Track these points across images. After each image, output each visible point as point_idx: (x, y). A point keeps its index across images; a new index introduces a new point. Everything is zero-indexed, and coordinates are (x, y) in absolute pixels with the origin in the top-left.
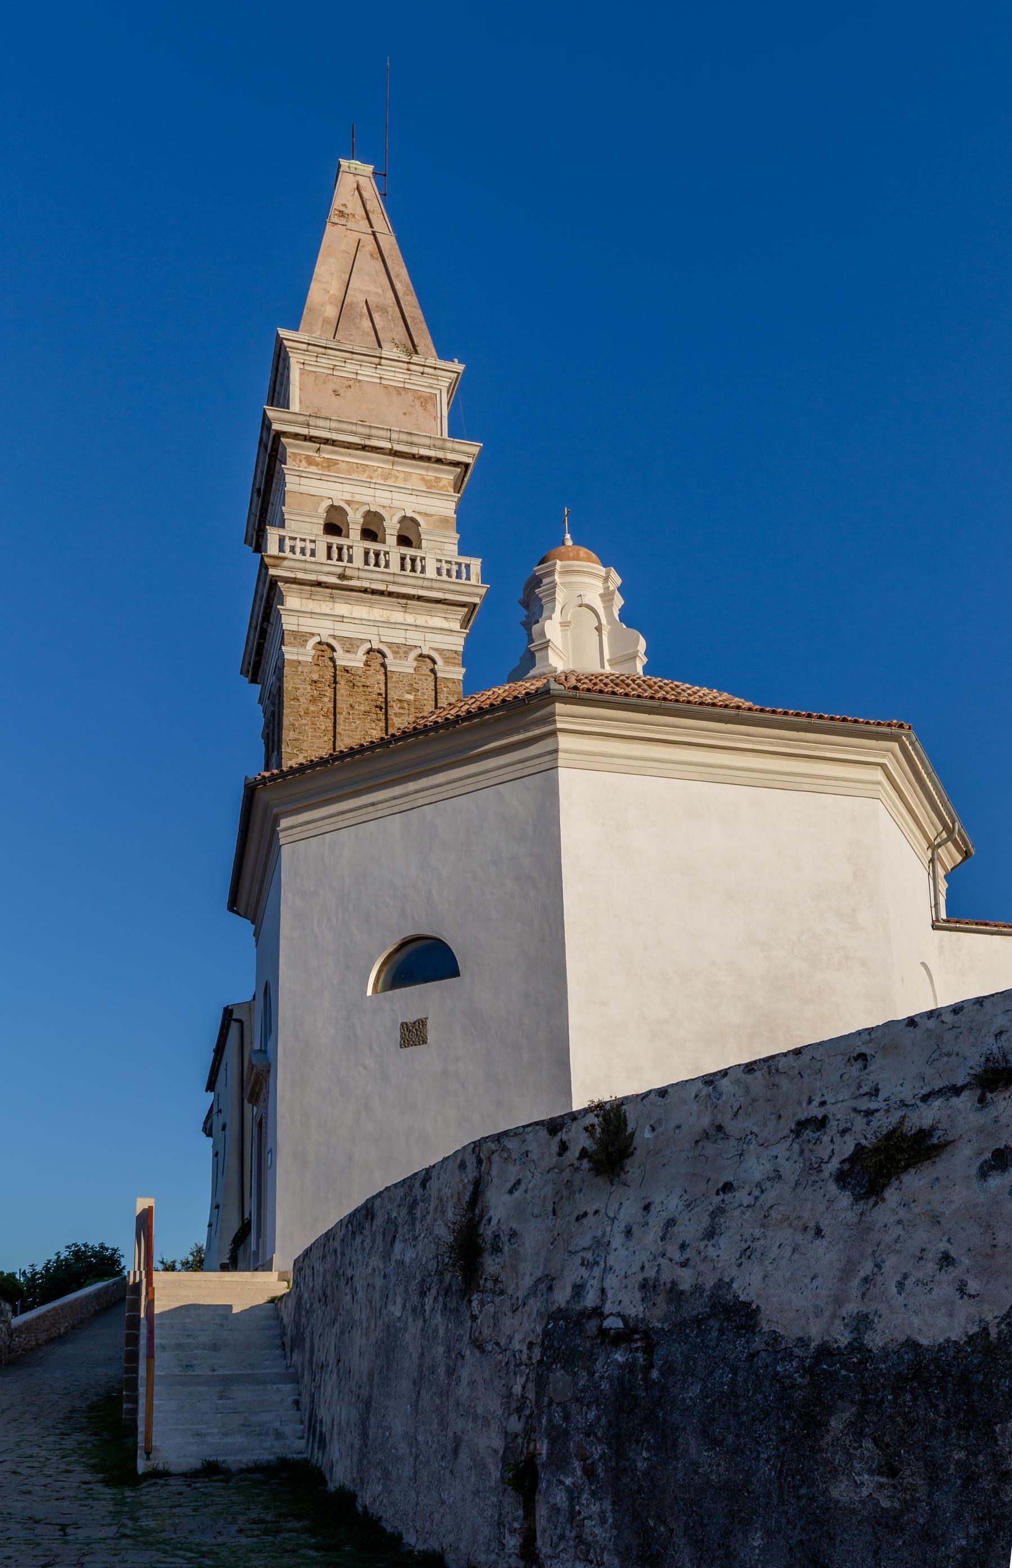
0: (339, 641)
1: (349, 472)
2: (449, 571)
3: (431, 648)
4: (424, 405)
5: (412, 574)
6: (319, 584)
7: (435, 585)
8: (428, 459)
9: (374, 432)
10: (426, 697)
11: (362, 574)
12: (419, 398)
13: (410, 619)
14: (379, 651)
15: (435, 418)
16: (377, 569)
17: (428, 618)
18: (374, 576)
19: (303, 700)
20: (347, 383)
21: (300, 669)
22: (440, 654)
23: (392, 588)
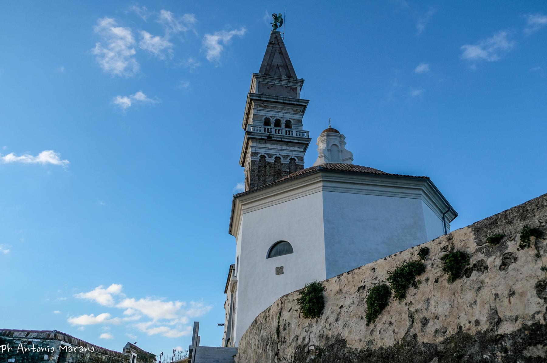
0: (267, 155)
1: (271, 109)
2: (300, 134)
3: (294, 156)
4: (293, 90)
5: (289, 136)
7: (296, 138)
9: (278, 98)
10: (293, 170)
11: (274, 136)
12: (292, 88)
13: (288, 148)
14: (279, 157)
15: (296, 94)
16: (279, 134)
17: (294, 148)
18: (278, 136)
19: (256, 172)
20: (271, 85)
21: (255, 163)
22: (297, 158)
23: (283, 140)
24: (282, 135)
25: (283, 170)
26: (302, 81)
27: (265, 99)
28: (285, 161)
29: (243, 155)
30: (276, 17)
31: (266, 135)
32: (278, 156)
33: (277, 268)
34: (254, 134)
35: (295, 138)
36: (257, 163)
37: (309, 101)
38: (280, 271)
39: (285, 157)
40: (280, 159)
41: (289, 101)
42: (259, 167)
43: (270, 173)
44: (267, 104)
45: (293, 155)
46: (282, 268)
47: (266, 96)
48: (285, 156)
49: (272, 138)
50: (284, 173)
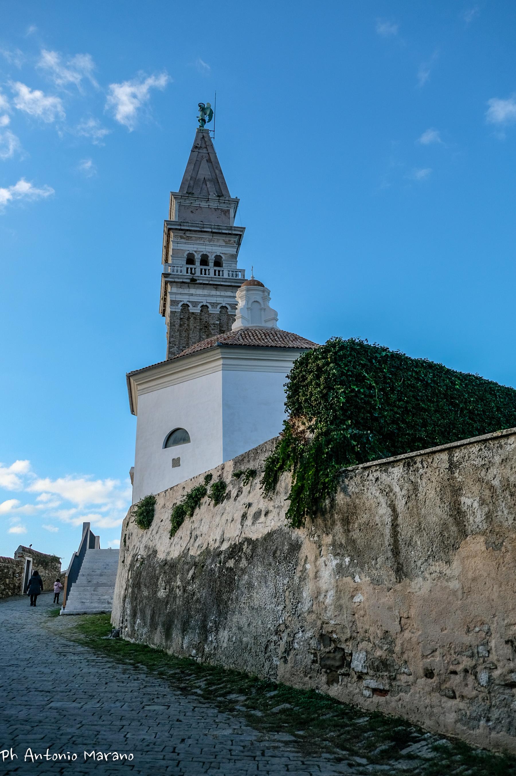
1: (196, 240)
2: (232, 274)
4: (225, 214)
5: (219, 277)
6: (183, 282)
7: (227, 280)
8: (226, 234)
9: (205, 226)
11: (200, 278)
13: (218, 293)
14: (206, 306)
15: (229, 218)
16: (205, 276)
17: (225, 292)
18: (204, 278)
23: (211, 282)
24: (209, 276)
25: (212, 322)
26: (236, 202)
27: (188, 228)
28: (215, 311)
29: (162, 302)
30: (203, 109)
31: (188, 277)
32: (205, 304)
33: (173, 459)
34: (173, 276)
35: (226, 280)
36: (178, 314)
37: (245, 228)
38: (176, 463)
39: (214, 305)
40: (208, 307)
41: (219, 229)
42: (181, 319)
43: (195, 327)
44: (190, 234)
45: (224, 302)
46: (179, 459)
47: (188, 224)
48: (214, 303)
49: (196, 280)
50: (212, 326)
